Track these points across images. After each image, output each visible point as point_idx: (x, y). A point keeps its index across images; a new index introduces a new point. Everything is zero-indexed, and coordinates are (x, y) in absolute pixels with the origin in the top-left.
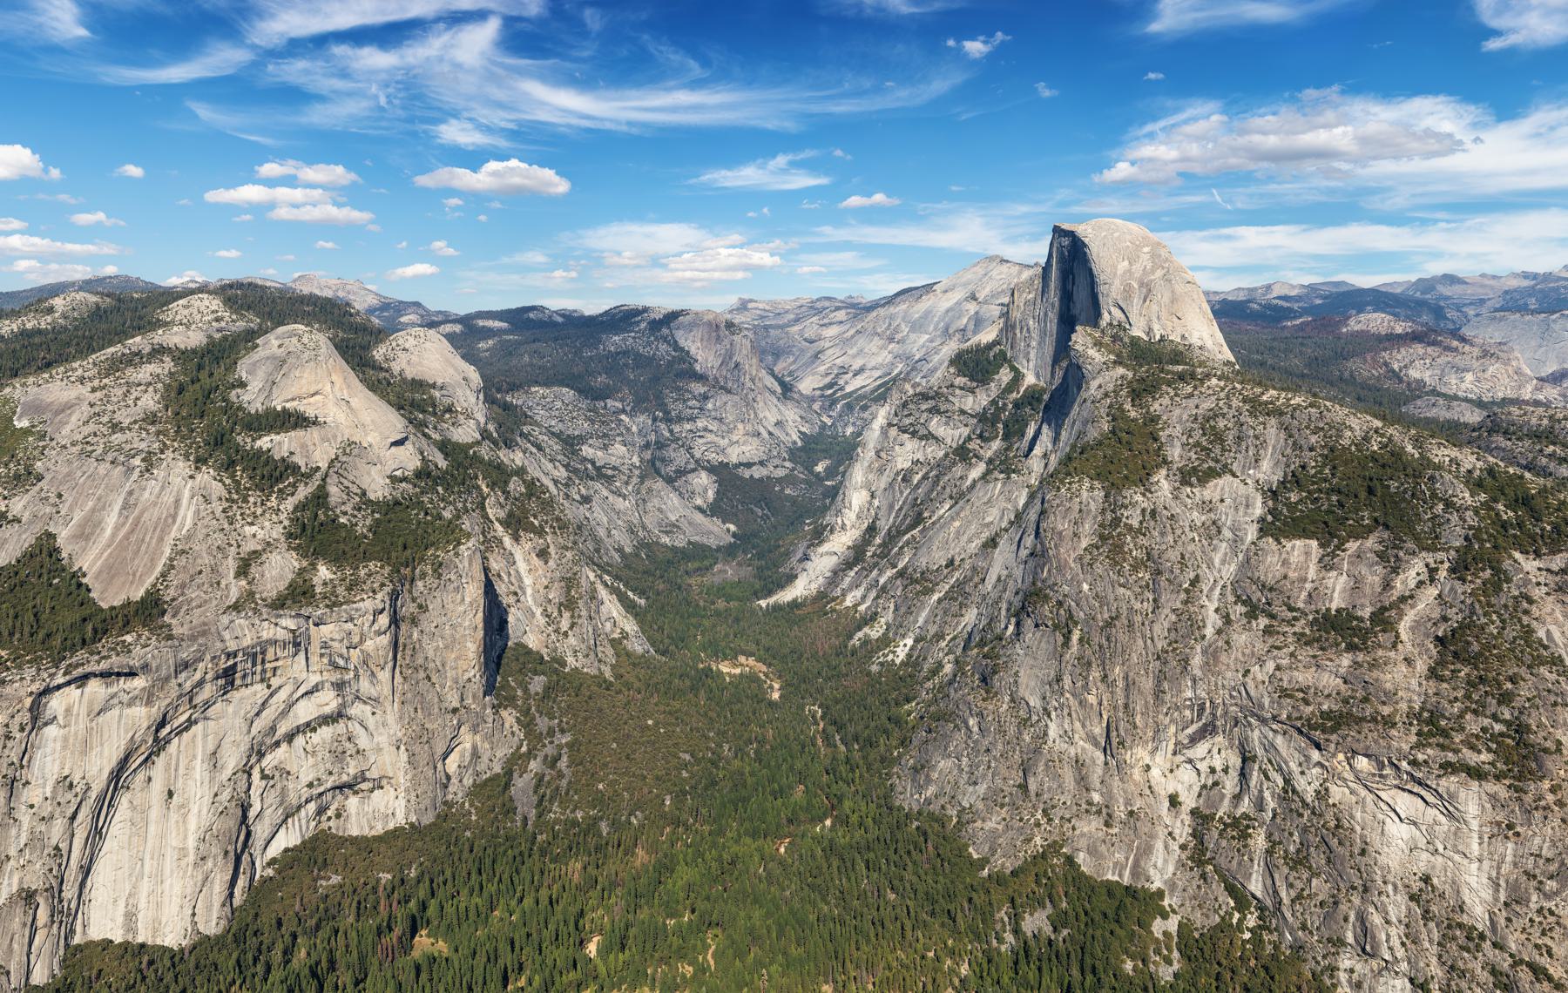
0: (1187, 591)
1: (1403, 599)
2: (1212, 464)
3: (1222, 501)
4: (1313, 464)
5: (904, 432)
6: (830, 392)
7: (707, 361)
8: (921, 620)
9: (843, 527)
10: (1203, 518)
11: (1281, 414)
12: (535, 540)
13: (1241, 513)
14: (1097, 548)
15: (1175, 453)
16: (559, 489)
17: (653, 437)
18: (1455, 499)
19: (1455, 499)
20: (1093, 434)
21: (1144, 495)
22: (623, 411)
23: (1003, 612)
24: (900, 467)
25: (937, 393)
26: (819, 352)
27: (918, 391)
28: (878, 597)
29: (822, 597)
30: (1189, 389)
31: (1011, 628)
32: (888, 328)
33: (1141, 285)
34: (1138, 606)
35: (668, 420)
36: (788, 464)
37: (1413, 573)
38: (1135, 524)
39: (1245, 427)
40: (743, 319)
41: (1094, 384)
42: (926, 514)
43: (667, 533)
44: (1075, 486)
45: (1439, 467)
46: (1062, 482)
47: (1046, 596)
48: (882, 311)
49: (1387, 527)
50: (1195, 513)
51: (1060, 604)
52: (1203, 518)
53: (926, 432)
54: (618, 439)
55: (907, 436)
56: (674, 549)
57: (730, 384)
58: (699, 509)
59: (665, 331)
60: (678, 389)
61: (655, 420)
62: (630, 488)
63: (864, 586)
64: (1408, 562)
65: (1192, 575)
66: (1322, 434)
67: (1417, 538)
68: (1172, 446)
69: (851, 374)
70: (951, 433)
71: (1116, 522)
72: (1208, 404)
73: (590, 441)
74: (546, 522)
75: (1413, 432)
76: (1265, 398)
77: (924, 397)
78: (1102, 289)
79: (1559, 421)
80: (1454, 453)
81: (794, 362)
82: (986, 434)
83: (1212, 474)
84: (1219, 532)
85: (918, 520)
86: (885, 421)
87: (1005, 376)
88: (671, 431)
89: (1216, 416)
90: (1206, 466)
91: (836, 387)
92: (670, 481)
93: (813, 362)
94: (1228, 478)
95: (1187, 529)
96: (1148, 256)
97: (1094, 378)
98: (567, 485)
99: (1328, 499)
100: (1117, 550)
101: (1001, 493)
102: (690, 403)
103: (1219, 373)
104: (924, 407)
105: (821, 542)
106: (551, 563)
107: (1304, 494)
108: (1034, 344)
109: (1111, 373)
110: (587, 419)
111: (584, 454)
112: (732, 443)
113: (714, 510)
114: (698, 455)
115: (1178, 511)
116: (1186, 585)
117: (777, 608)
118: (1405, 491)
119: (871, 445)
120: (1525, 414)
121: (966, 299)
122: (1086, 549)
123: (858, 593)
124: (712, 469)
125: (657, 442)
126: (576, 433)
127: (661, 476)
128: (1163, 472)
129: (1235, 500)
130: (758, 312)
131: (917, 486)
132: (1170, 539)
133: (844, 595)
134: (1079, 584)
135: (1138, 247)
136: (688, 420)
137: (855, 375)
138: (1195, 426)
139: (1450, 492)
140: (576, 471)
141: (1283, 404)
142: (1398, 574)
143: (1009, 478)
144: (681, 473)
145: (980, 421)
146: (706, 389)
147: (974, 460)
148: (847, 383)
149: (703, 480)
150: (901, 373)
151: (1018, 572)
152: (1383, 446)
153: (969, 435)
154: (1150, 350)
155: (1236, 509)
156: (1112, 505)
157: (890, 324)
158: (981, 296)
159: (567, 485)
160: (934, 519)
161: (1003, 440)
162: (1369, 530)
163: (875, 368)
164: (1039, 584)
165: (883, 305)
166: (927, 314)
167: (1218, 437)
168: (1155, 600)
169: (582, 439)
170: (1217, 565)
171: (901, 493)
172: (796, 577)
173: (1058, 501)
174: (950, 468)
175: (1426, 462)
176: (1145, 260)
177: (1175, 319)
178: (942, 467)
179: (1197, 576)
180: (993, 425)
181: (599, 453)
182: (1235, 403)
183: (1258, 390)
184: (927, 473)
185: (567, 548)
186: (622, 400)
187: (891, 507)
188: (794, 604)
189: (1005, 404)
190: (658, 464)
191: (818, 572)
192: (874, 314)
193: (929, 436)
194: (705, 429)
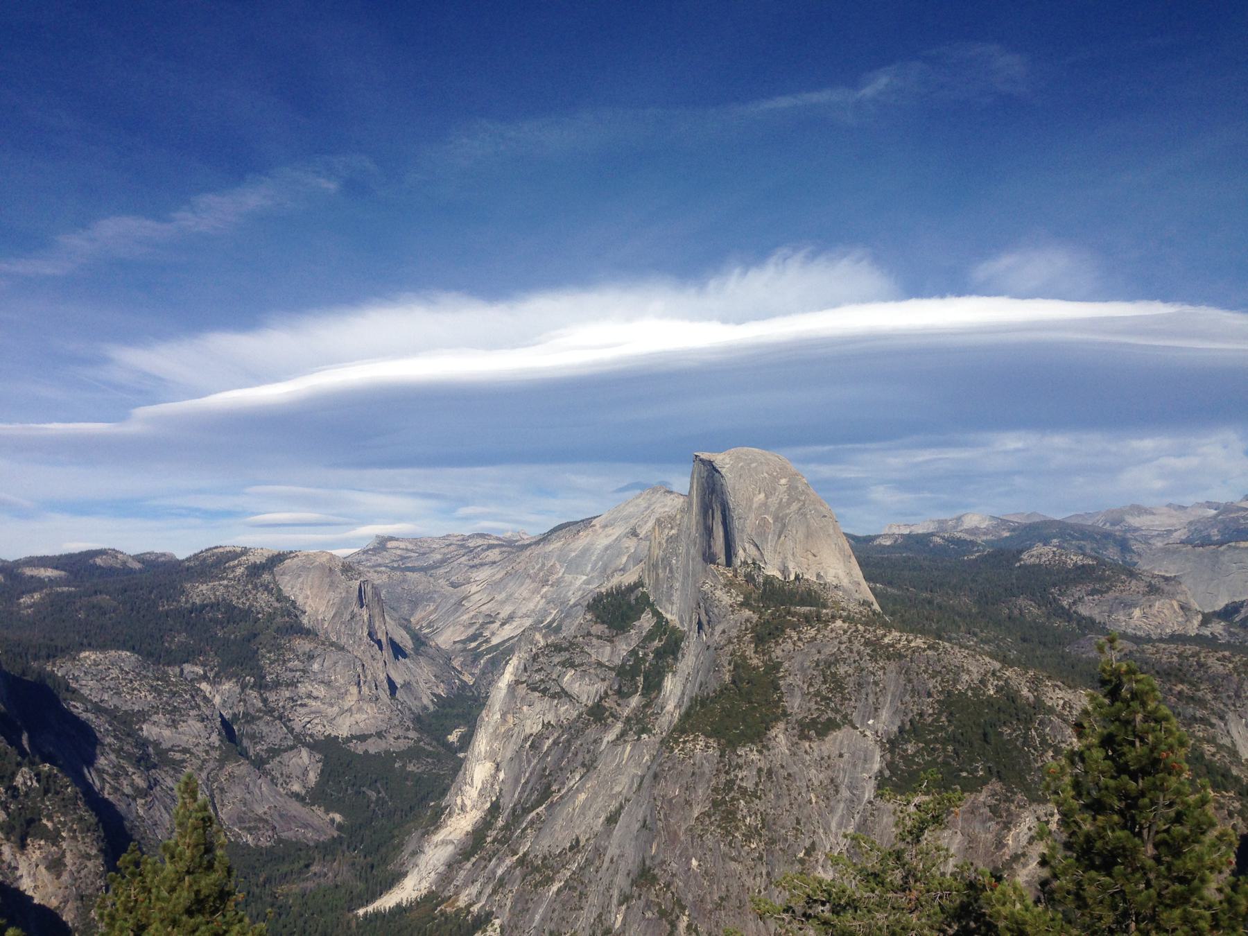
0: (802, 861)
1: (1016, 858)
2: (831, 714)
3: (841, 756)
4: (931, 711)
5: (534, 689)
6: (473, 645)
7: (317, 611)
8: (537, 917)
9: (463, 808)
10: (821, 776)
11: (901, 656)
12: (46, 849)
13: (859, 769)
14: (710, 817)
15: (795, 704)
16: (103, 780)
17: (242, 709)
18: (1063, 745)
19: (1063, 745)
20: (714, 685)
21: (760, 752)
22: (204, 677)
23: (615, 901)
24: (528, 731)
25: (571, 644)
26: (464, 598)
27: (549, 641)
28: (495, 892)
29: (430, 900)
30: (813, 632)
31: (620, 918)
32: (540, 569)
33: (776, 519)
34: (749, 882)
35: (261, 685)
36: (412, 734)
37: (1024, 828)
38: (749, 785)
39: (864, 673)
40: (380, 561)
41: (719, 629)
42: (554, 788)
43: (249, 830)
44: (689, 745)
45: (1051, 710)
46: (676, 742)
47: (654, 876)
48: (536, 550)
49: (1000, 778)
50: (813, 771)
51: (668, 886)
52: (821, 776)
53: (558, 690)
54: (192, 713)
55: (537, 694)
56: (259, 850)
57: (343, 641)
58: (296, 795)
59: (266, 577)
60: (279, 647)
61: (243, 688)
62: (204, 775)
63: (481, 880)
64: (1018, 816)
65: (807, 843)
66: (939, 679)
67: (1027, 790)
68: (792, 696)
69: (497, 624)
70: (585, 689)
71: (730, 784)
72: (831, 649)
73: (155, 718)
74: (64, 824)
75: (1031, 673)
76: (886, 640)
77: (558, 648)
78: (737, 524)
79: (1187, 658)
80: (1068, 695)
81: (436, 609)
82: (625, 689)
83: (831, 725)
84: (837, 792)
85: (546, 793)
86: (513, 678)
87: (646, 621)
88: (265, 701)
89: (837, 661)
90: (825, 717)
91: (480, 640)
92: (259, 764)
93: (456, 610)
94: (846, 729)
95: (804, 790)
96: (785, 488)
97: (719, 622)
98: (116, 776)
99: (945, 750)
100: (730, 816)
101: (630, 757)
102: (289, 665)
103: (845, 614)
104: (556, 660)
105: (437, 828)
106: (65, 877)
107: (921, 745)
108: (677, 585)
109: (736, 617)
110: (153, 689)
111: (145, 733)
112: (342, 712)
113: (316, 796)
114: (298, 729)
115: (795, 769)
116: (802, 855)
117: (377, 915)
118: (1016, 739)
119: (497, 707)
120: (1157, 652)
121: (626, 536)
122: (697, 818)
123: (473, 890)
124: (315, 746)
125: (246, 714)
126: (136, 708)
127: (247, 757)
128: (781, 725)
129: (853, 754)
130: (399, 552)
131: (547, 754)
132: (786, 801)
133: (457, 894)
134: (688, 862)
135: (775, 479)
136: (288, 685)
137: (503, 624)
138: (815, 673)
139: (1059, 738)
140: (129, 757)
141: (904, 646)
142: (1010, 830)
143: (639, 738)
144: (274, 752)
145: (617, 675)
146: (312, 646)
147: (611, 719)
148: (493, 634)
149: (304, 761)
150: (554, 620)
151: (630, 852)
152: (999, 690)
153: (606, 693)
154: (784, 590)
155: (855, 765)
156: (726, 766)
157: (543, 565)
158: (642, 533)
159: (116, 776)
160: (563, 791)
161: (642, 694)
162: (984, 782)
163: (526, 616)
164: (647, 863)
165: (537, 543)
166: (586, 551)
167: (838, 684)
168: (768, 874)
169: (143, 716)
170: (833, 829)
171: (529, 762)
172: (405, 875)
173: (670, 764)
174: (583, 730)
175: (1039, 705)
176: (781, 493)
177: (810, 556)
178: (574, 730)
179: (813, 843)
180: (633, 678)
181: (167, 733)
182: (857, 646)
183: (880, 632)
184: (559, 737)
185: (88, 857)
186: (204, 665)
187: (517, 780)
188: (399, 910)
189: (646, 654)
190: (246, 742)
191: (430, 867)
192: (528, 552)
193: (563, 694)
194: (309, 696)
